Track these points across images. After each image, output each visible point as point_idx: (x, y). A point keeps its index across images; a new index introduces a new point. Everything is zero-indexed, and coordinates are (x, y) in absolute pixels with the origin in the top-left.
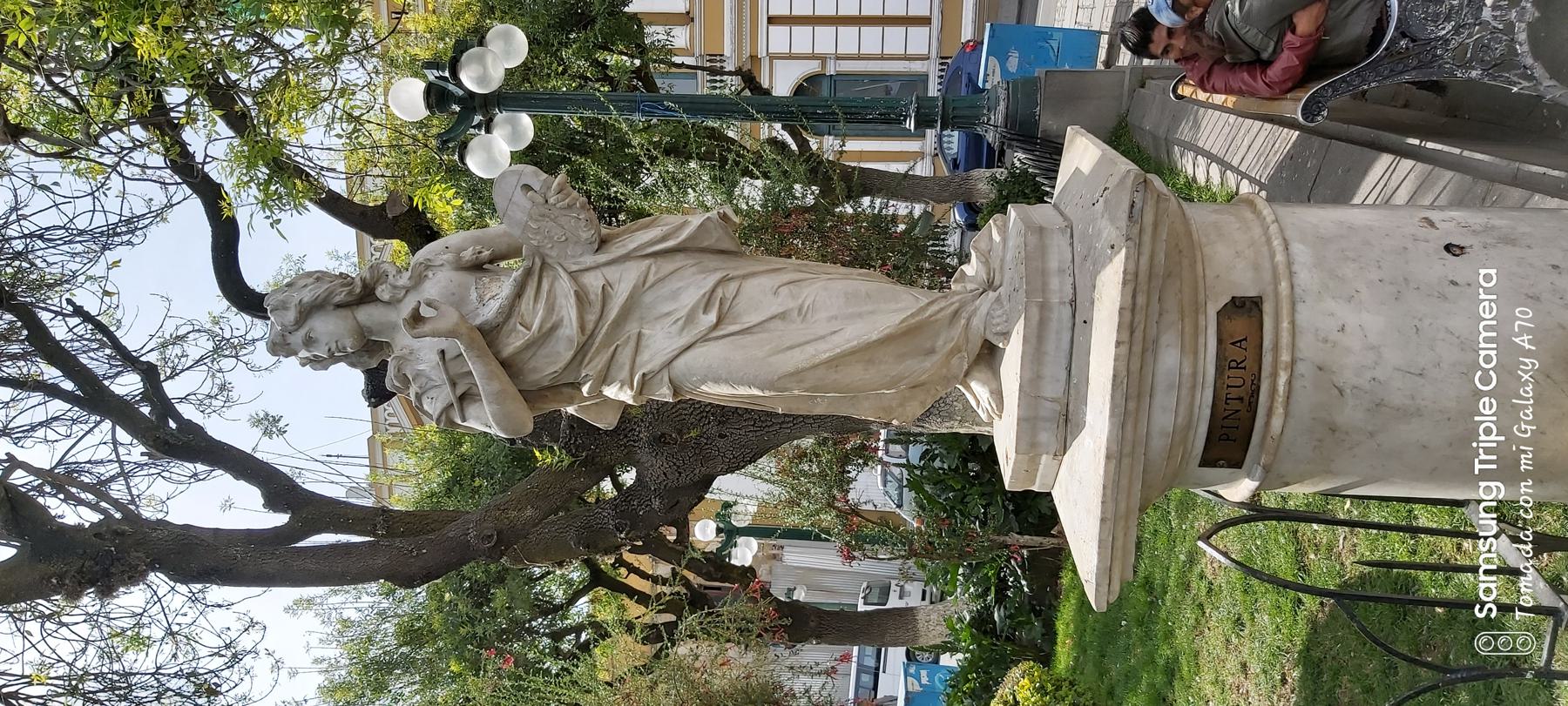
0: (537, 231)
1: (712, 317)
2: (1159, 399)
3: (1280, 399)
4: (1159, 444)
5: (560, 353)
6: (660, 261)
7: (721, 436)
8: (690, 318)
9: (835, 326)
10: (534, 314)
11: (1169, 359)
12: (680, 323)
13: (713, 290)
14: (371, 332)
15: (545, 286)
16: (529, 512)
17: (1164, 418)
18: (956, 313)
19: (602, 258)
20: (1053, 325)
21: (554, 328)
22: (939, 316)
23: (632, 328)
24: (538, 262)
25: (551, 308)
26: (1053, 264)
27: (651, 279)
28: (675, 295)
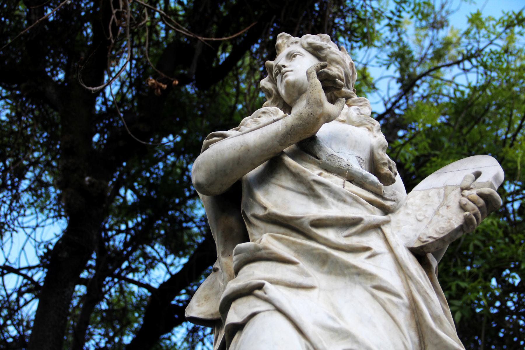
12: (331, 323)
24: (388, 204)
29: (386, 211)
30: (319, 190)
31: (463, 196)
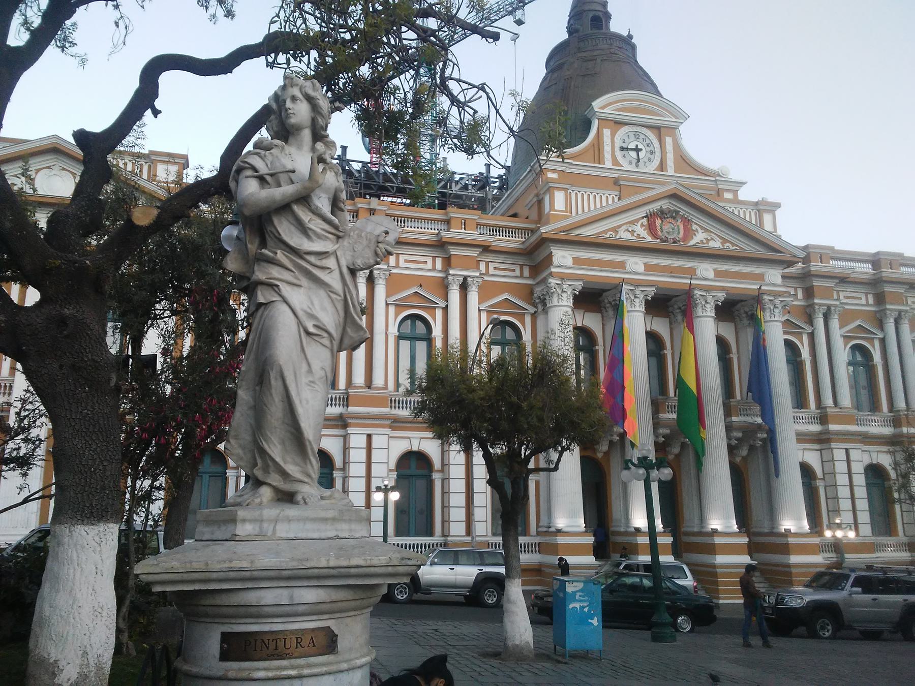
0: (360, 236)
1: (312, 330)
2: (285, 592)
3: (278, 673)
4: (252, 598)
6: (342, 303)
7: (61, 367)
8: (312, 316)
9: (304, 402)
10: (316, 225)
11: (309, 595)
12: (309, 311)
15: (330, 236)
16: (8, 225)
17: (270, 596)
18: (309, 476)
19: (345, 270)
21: (308, 237)
22: (309, 466)
23: (304, 281)
24: (341, 234)
25: (319, 237)
26: (353, 526)
27: (333, 296)
28: (324, 309)
29: (339, 237)
30: (310, 233)
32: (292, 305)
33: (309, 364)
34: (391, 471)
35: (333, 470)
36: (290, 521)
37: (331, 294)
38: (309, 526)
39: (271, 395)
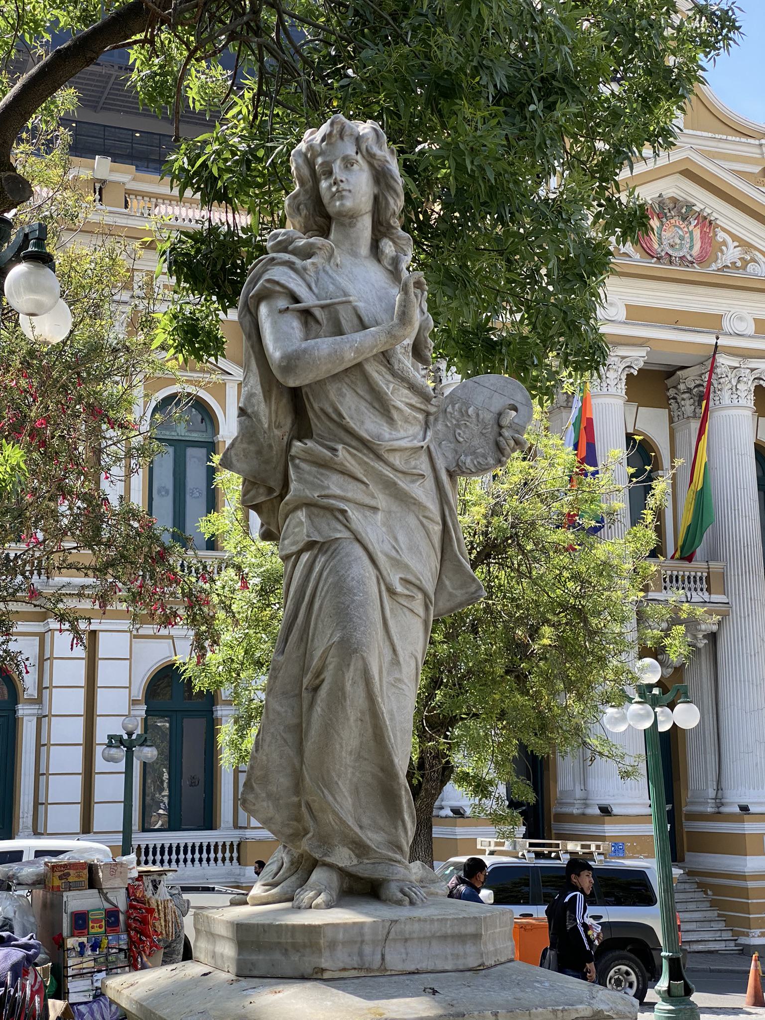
0: (464, 414)
5: (369, 425)
12: (394, 554)
13: (420, 589)
14: (352, 225)
20: (459, 949)
21: (390, 420)
23: (382, 500)
28: (413, 548)
30: (395, 415)
31: (500, 435)
32: (370, 547)
33: (394, 651)
34: (134, 702)
35: (16, 702)
36: (406, 940)
37: (424, 521)
38: (437, 948)
39: (344, 708)
